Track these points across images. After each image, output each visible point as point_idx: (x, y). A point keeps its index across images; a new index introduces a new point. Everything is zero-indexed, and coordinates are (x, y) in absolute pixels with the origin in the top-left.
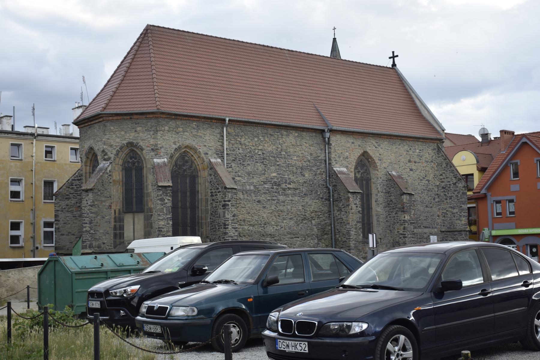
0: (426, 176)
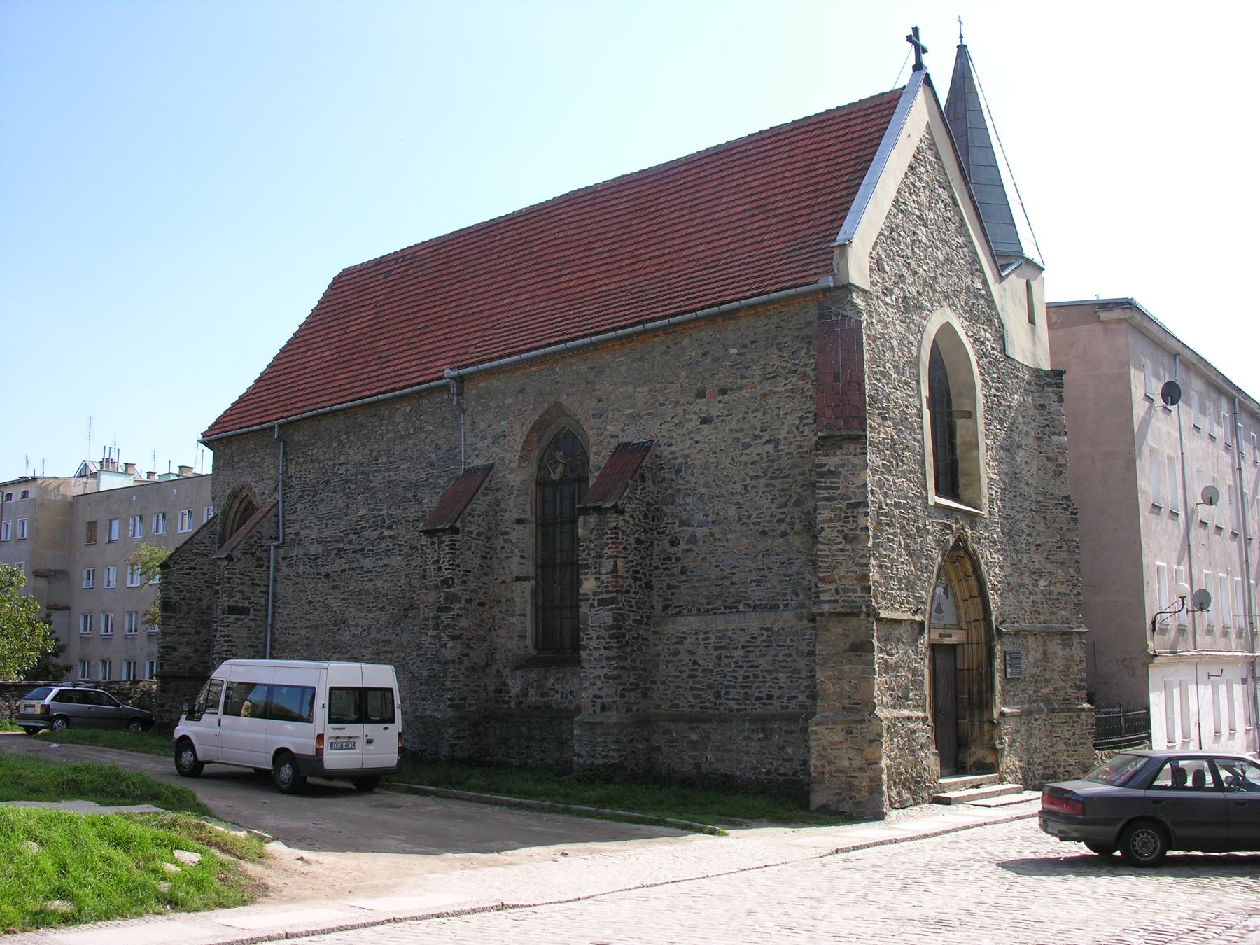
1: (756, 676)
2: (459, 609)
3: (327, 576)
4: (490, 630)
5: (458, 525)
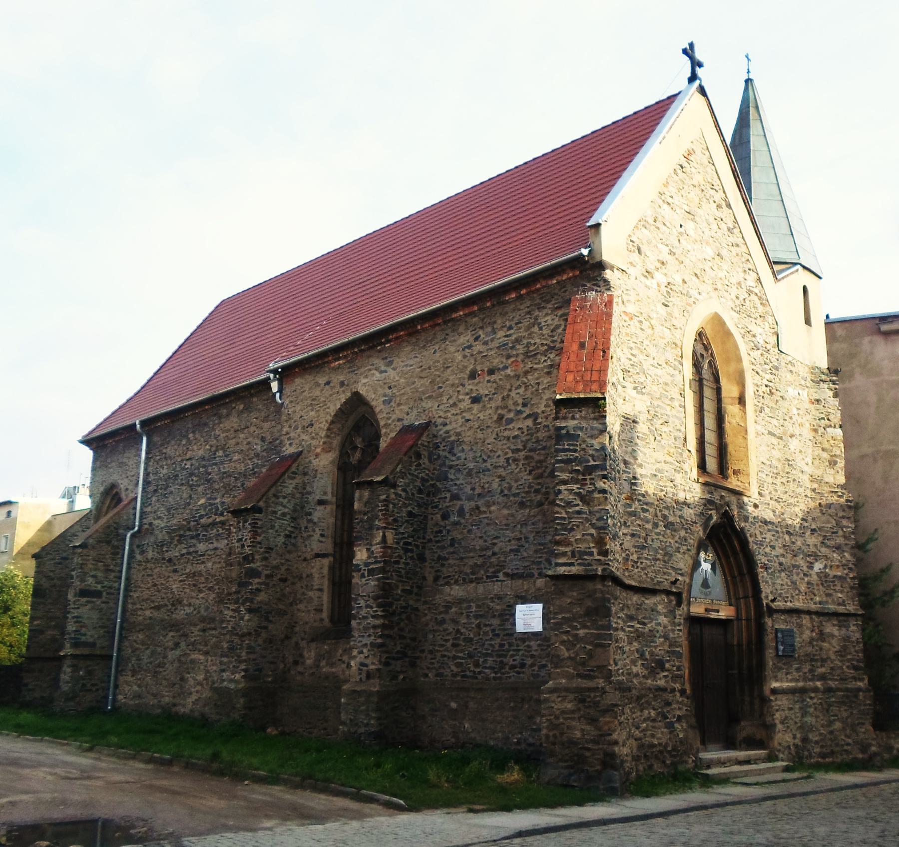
0: (525, 405)
1: (510, 645)
2: (258, 583)
3: (170, 560)
4: (291, 604)
5: (261, 504)
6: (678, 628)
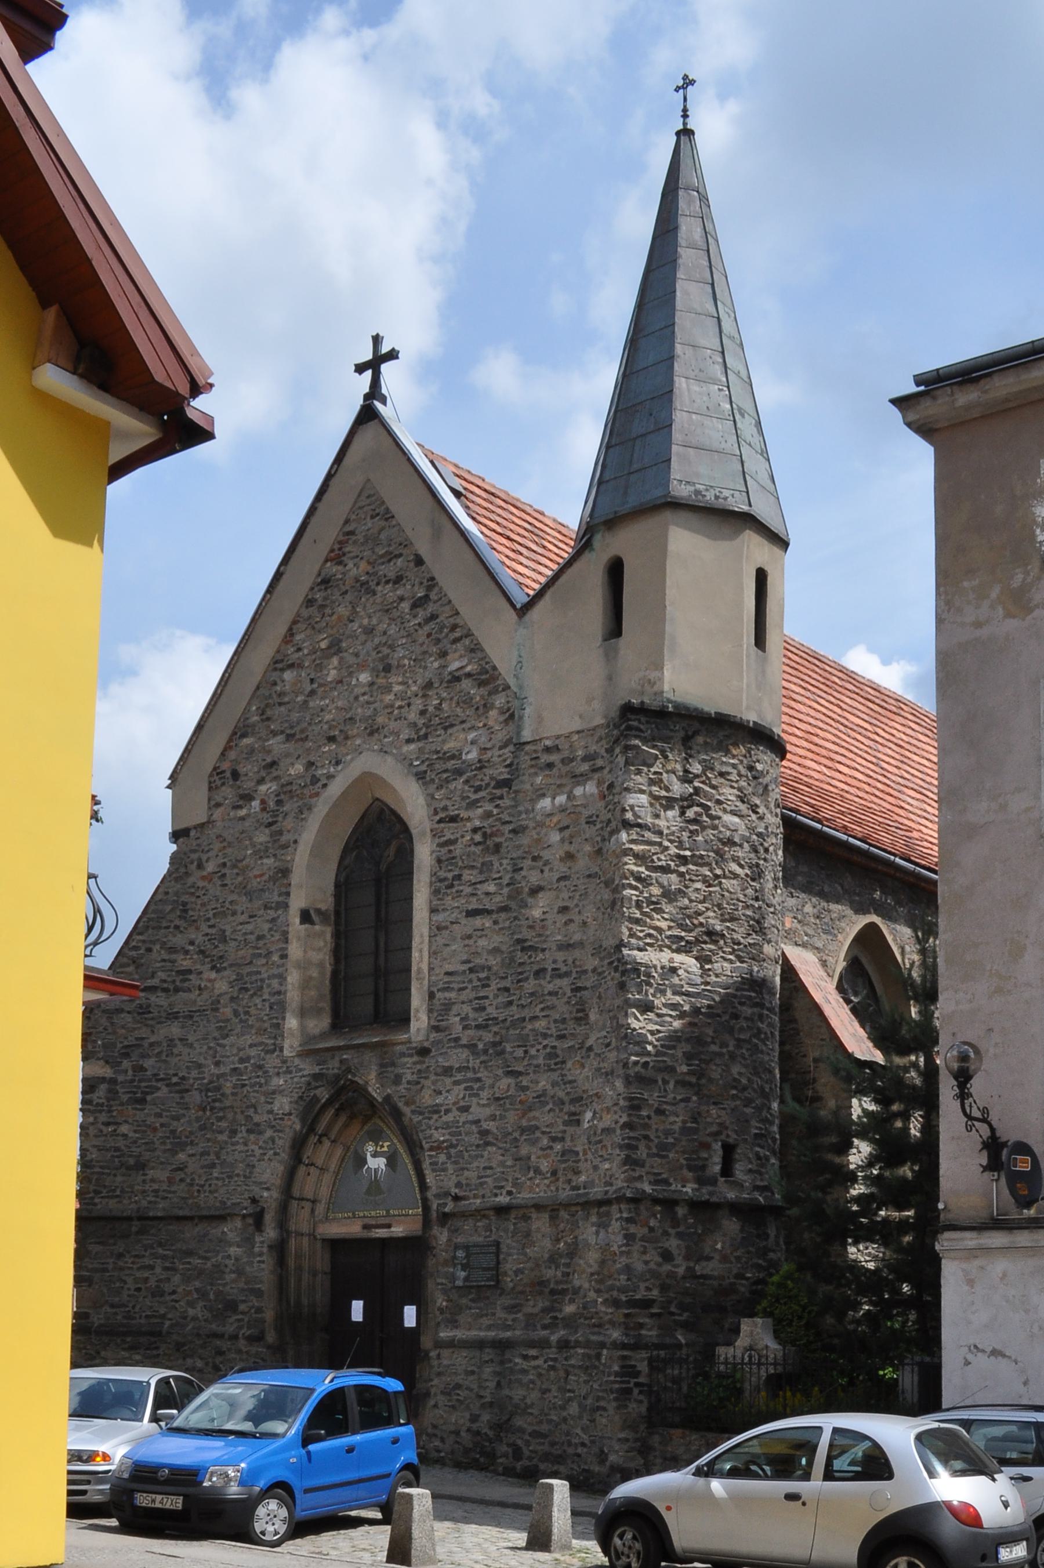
6: (258, 1259)
